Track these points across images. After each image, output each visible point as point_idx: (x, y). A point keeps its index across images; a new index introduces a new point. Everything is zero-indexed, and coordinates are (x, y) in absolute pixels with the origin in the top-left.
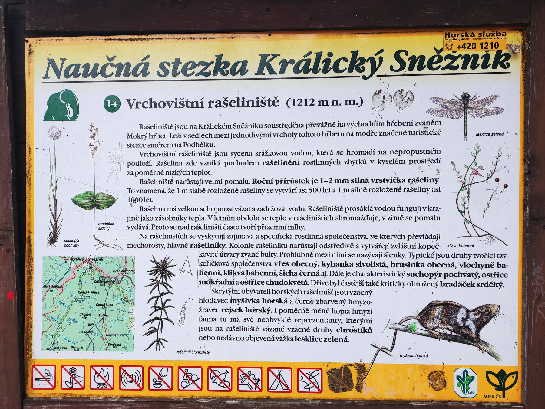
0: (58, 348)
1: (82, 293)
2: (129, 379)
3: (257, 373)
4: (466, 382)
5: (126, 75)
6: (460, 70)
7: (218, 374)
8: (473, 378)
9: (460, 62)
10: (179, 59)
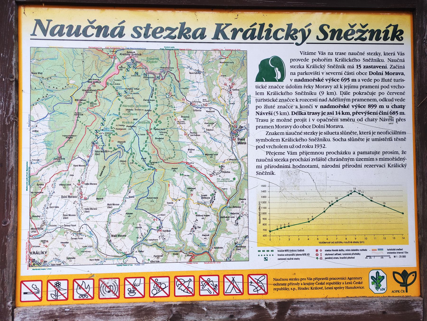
2: (108, 290)
4: (378, 281)
5: (105, 36)
6: (367, 41)
7: (183, 283)
8: (383, 277)
9: (367, 35)
10: (150, 25)
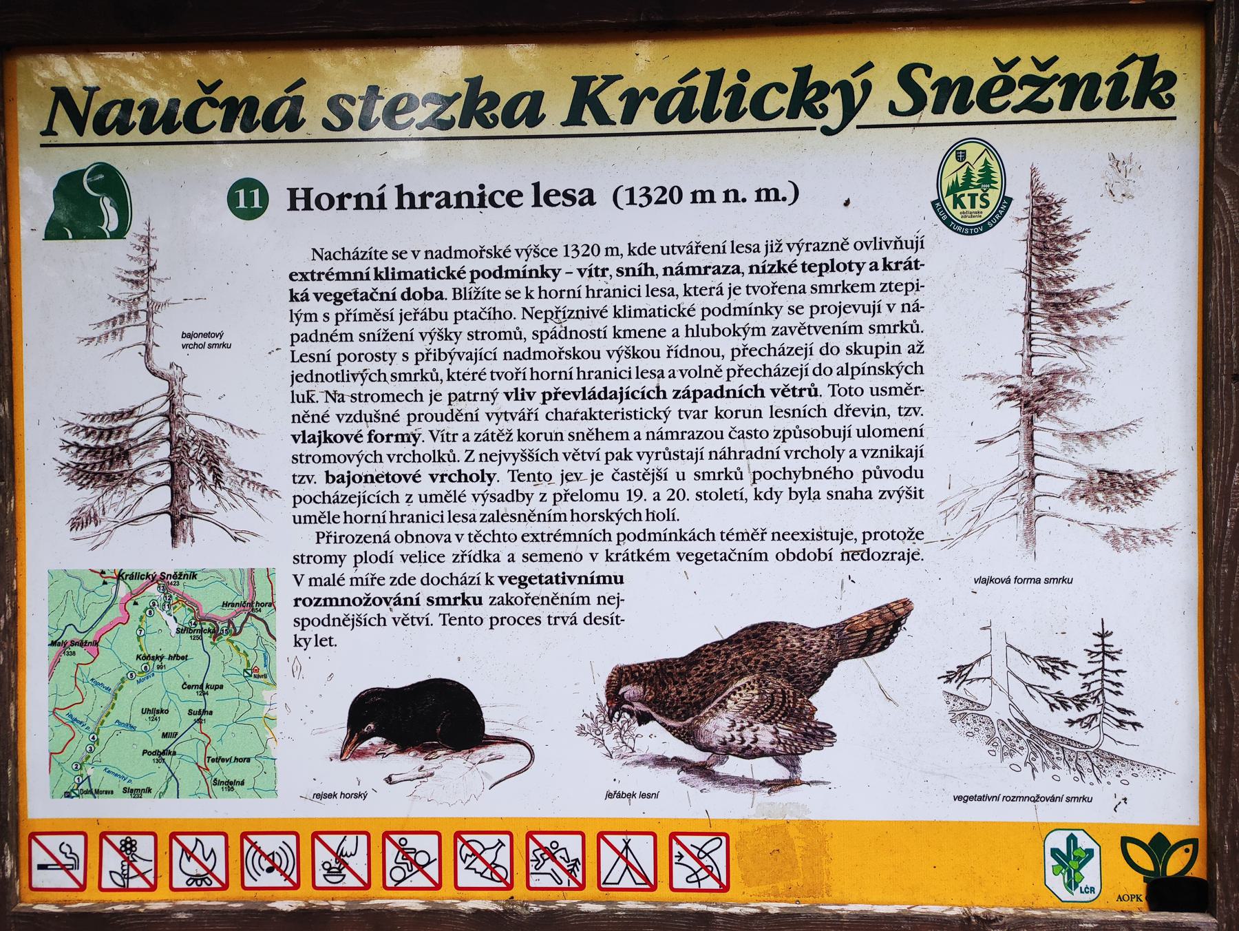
0: (90, 792)
1: (147, 657)
2: (266, 864)
3: (572, 845)
4: (1074, 864)
6: (1055, 113)
7: (479, 849)
8: (1090, 852)
9: (1055, 93)
